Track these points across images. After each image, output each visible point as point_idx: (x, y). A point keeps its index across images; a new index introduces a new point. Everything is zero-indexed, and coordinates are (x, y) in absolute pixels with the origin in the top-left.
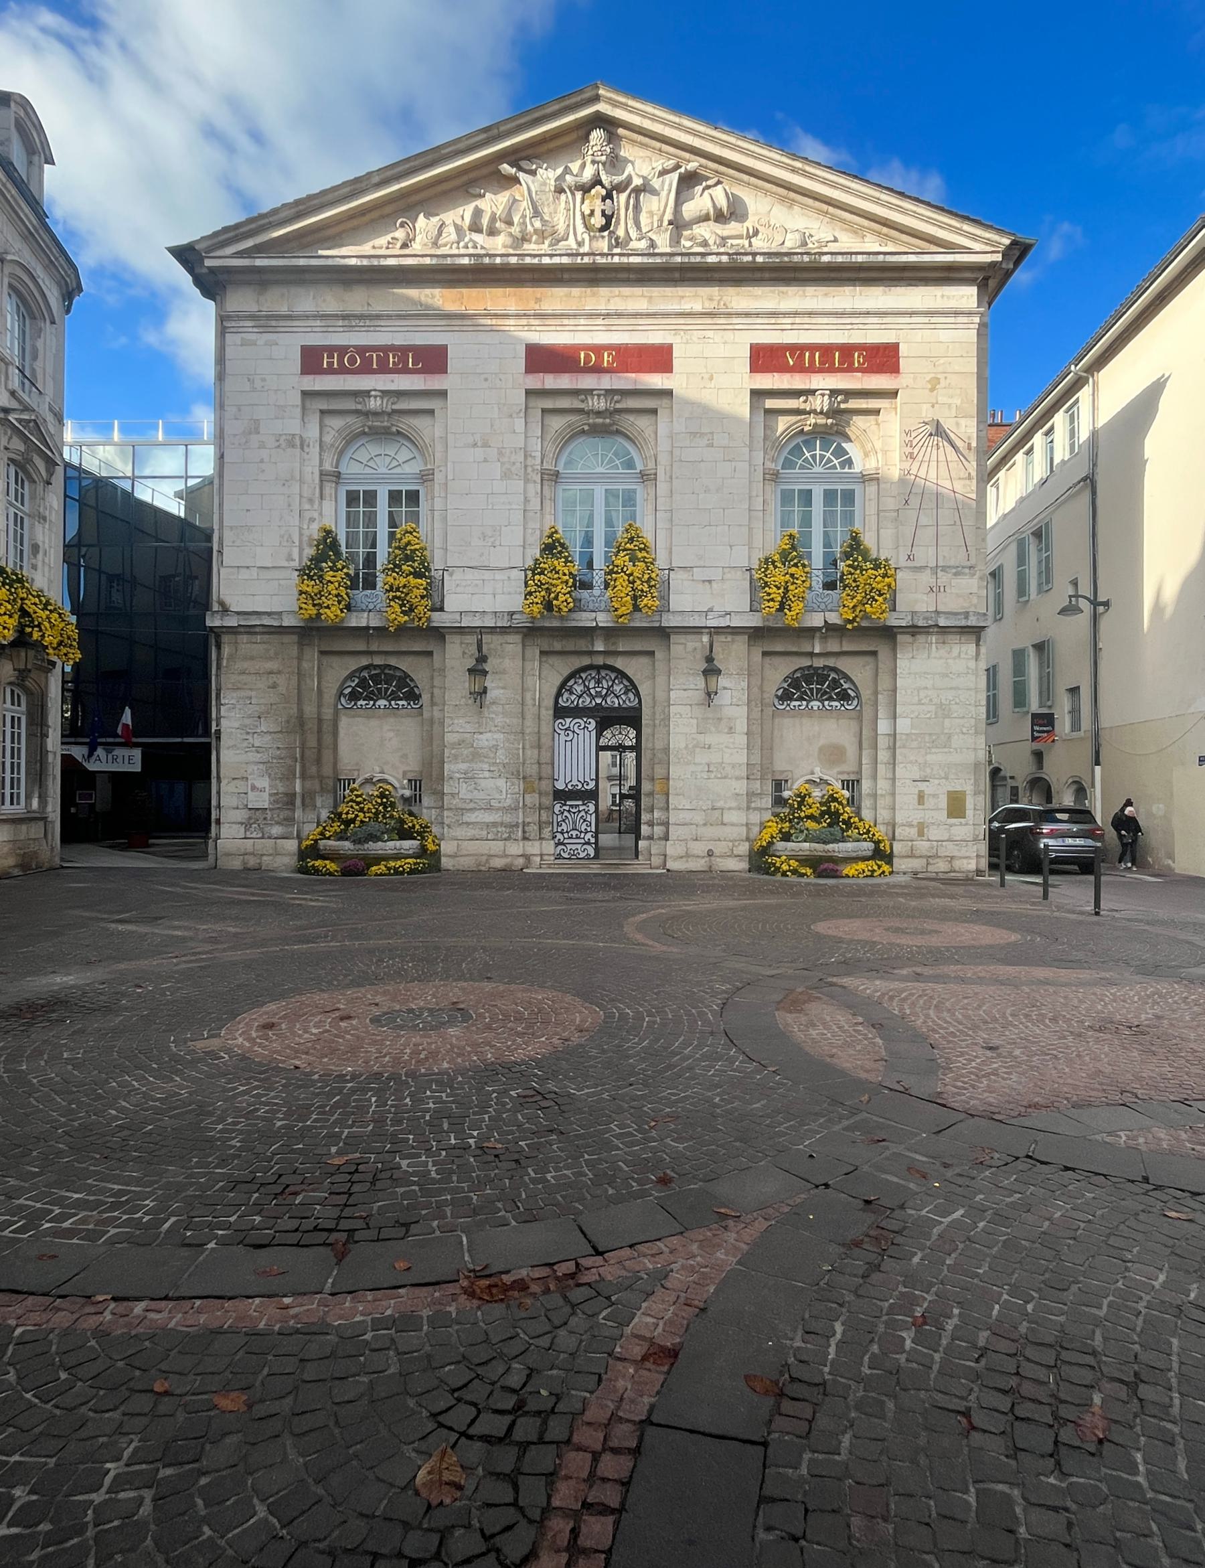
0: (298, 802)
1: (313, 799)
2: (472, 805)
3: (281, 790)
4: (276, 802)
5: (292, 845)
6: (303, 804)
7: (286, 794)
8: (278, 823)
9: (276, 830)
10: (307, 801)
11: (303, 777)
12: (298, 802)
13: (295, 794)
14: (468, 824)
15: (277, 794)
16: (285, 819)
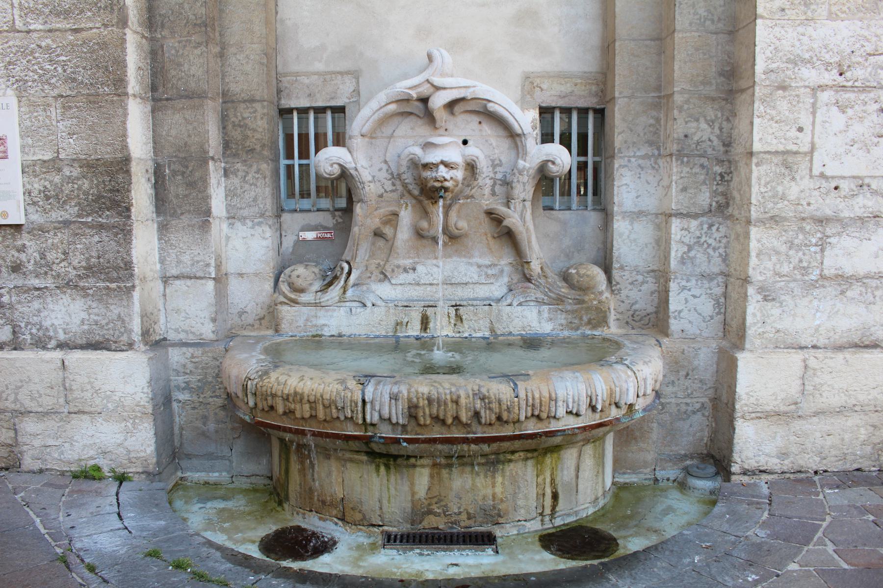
0: (141, 195)
1: (198, 186)
2: (864, 204)
3: (71, 147)
4: (51, 197)
5: (126, 377)
6: (161, 201)
7: (90, 166)
8: (68, 285)
9: (66, 313)
10: (175, 189)
11: (161, 92)
12: (141, 195)
13: (124, 163)
14: (844, 281)
15: (53, 165)
16: (90, 270)
